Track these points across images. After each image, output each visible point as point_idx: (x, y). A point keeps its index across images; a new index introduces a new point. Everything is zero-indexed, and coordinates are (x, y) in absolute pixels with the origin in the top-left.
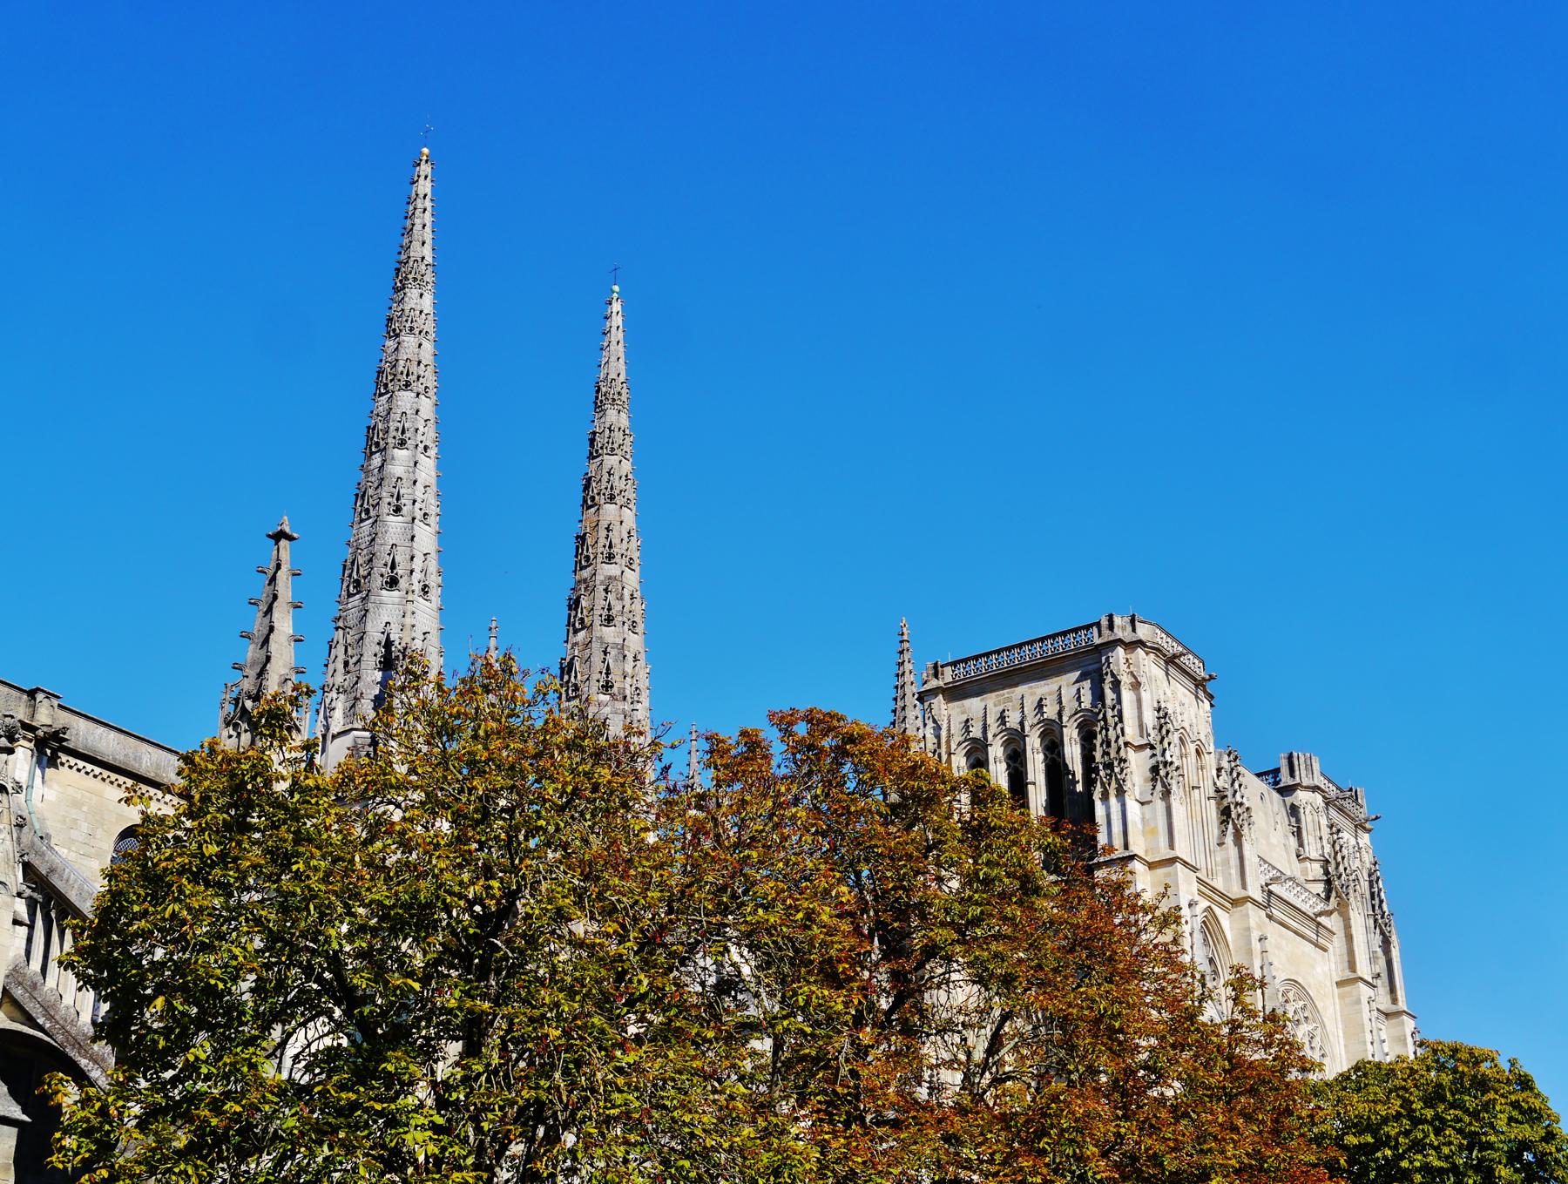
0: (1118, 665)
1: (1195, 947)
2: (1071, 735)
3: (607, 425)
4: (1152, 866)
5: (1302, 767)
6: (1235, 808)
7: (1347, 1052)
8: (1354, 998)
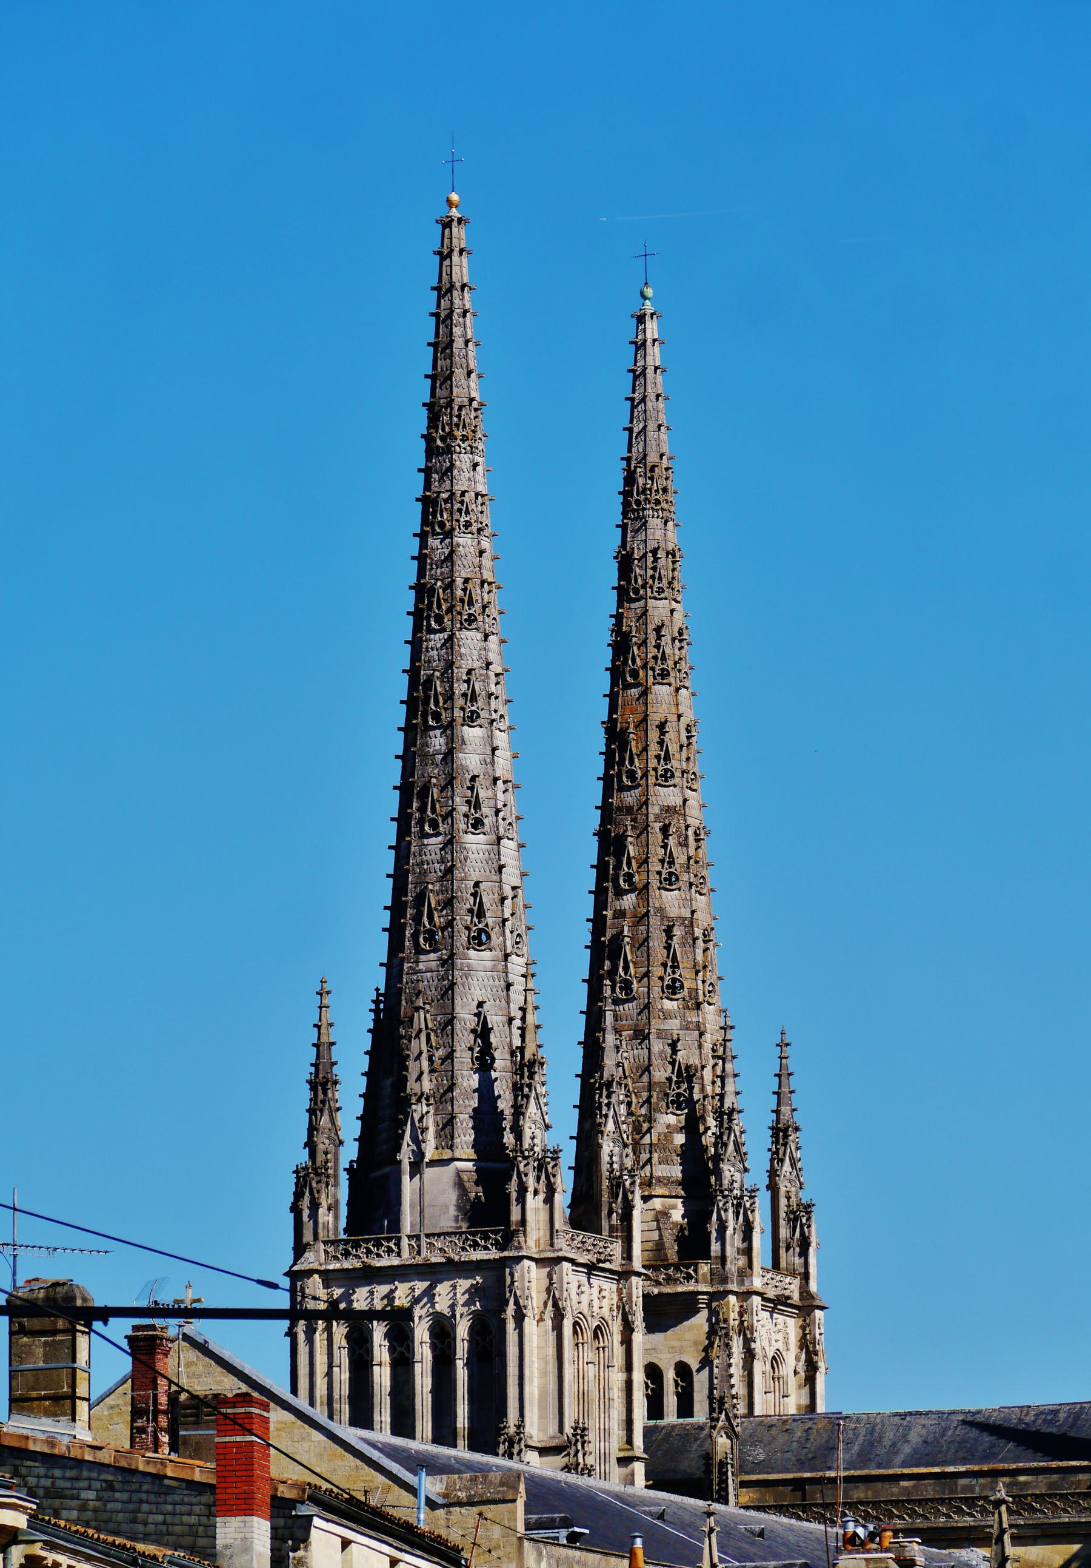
3: (652, 545)
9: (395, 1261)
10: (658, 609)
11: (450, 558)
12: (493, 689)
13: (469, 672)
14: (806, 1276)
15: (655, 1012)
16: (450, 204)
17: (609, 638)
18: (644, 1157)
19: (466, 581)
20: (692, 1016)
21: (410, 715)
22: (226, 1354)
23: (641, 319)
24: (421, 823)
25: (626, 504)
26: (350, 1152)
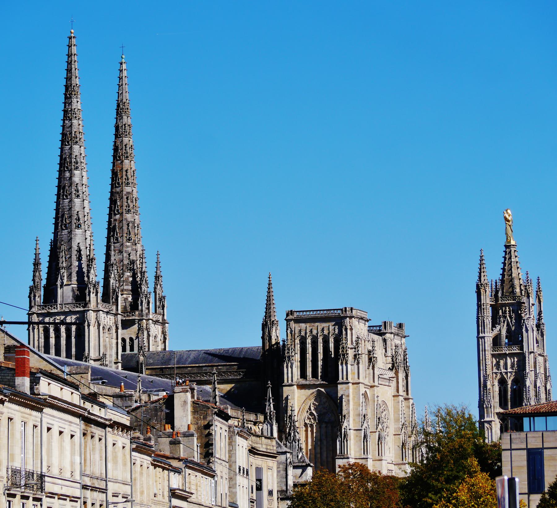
0: (347, 323)
2: (332, 340)
3: (124, 123)
4: (353, 384)
5: (389, 326)
8: (397, 401)
9: (56, 311)
10: (126, 140)
11: (71, 126)
12: (82, 161)
13: (76, 156)
14: (164, 315)
15: (124, 246)
16: (71, 33)
17: (112, 148)
18: (121, 284)
19: (75, 132)
20: (134, 247)
21: (60, 167)
22: (12, 335)
23: (121, 64)
24: (63, 196)
25: (117, 112)
26: (44, 282)
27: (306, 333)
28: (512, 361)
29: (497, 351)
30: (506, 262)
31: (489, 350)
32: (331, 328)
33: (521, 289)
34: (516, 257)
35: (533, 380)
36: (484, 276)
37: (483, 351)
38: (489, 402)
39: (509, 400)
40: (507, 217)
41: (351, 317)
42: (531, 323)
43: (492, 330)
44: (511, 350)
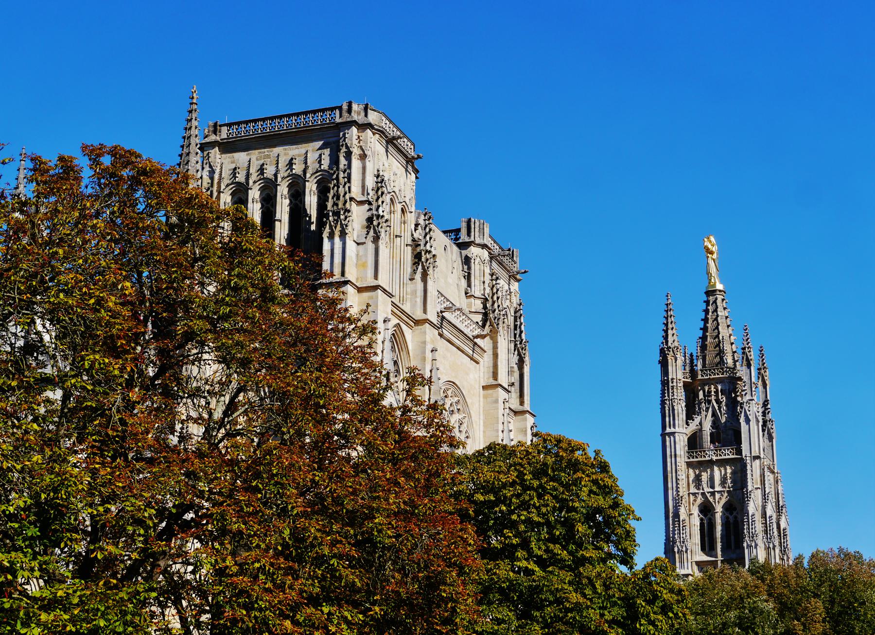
0: (352, 140)
1: (385, 351)
2: (311, 187)
4: (360, 290)
5: (477, 230)
6: (425, 254)
7: (484, 436)
8: (494, 399)
27: (248, 176)
28: (723, 473)
29: (697, 457)
30: (709, 317)
31: (683, 456)
32: (312, 157)
33: (734, 359)
34: (725, 309)
35: (760, 504)
36: (673, 335)
37: (673, 457)
38: (683, 542)
39: (719, 540)
40: (710, 246)
41: (364, 127)
42: (754, 409)
43: (687, 424)
44: (720, 455)
